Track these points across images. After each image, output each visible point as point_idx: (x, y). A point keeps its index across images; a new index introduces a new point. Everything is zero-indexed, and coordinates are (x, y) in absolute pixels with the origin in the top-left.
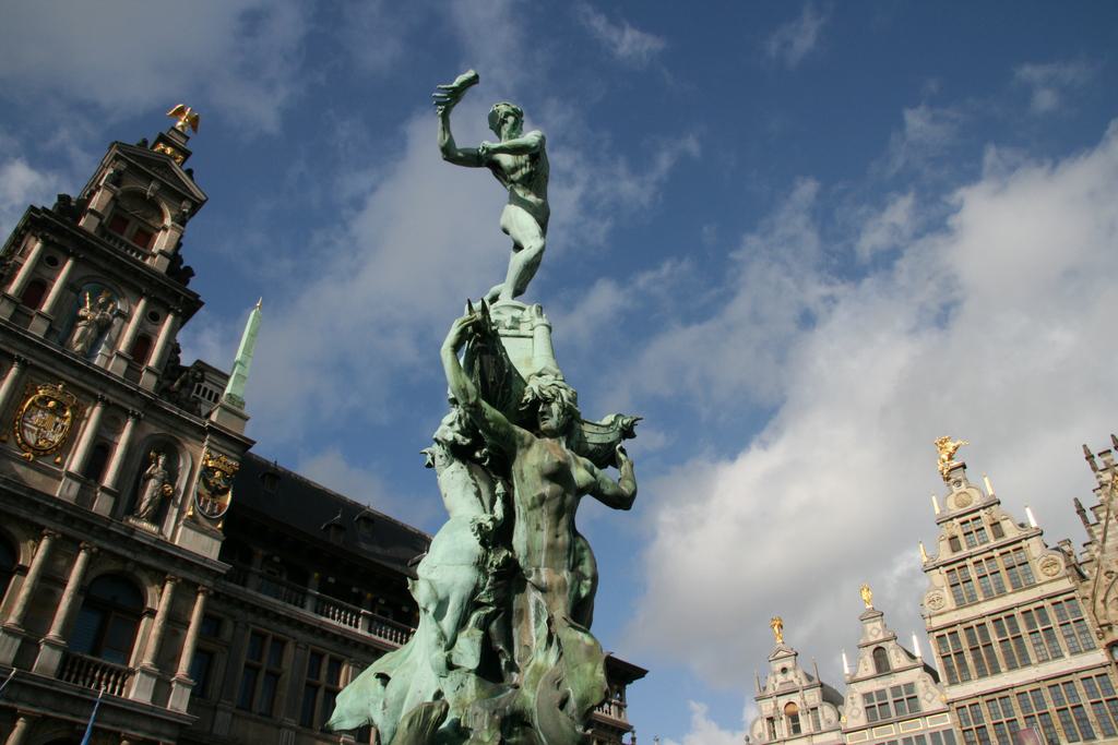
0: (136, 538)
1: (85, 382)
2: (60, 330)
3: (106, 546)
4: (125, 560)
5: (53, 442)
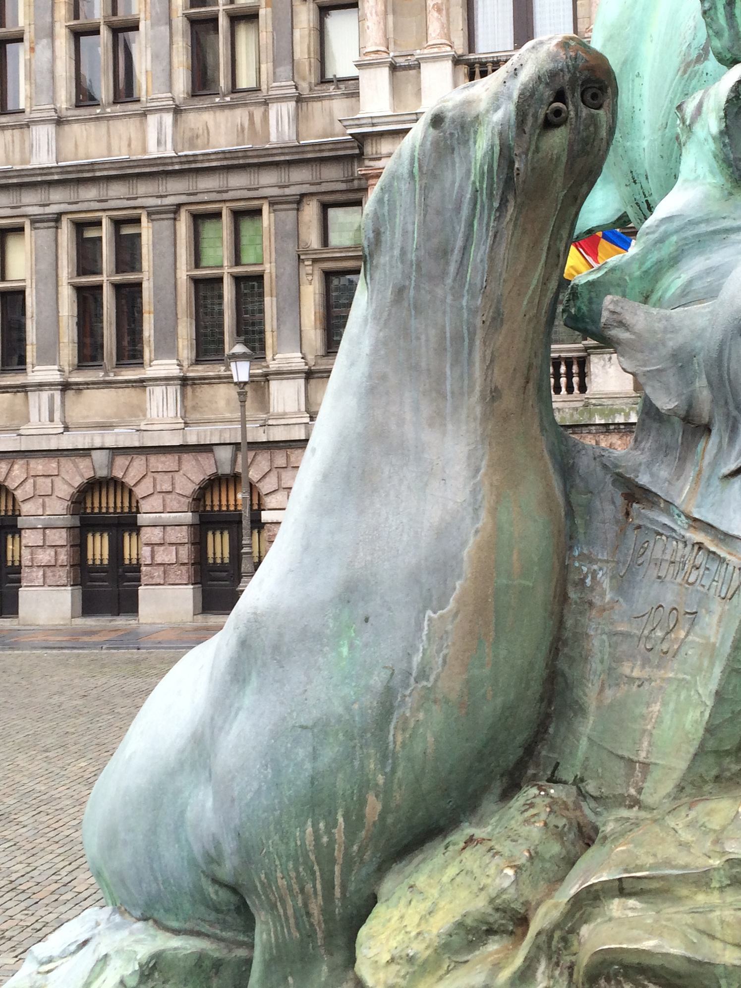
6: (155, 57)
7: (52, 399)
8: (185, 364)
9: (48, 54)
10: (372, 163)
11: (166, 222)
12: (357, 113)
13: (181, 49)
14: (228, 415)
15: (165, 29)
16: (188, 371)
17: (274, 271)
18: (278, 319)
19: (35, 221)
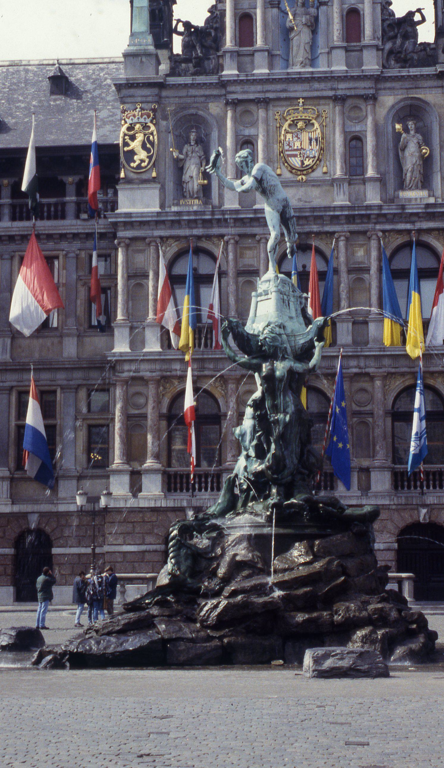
0: (407, 211)
1: (317, 90)
2: (278, 53)
3: (388, 227)
4: (409, 231)
5: (314, 157)
8: (12, 470)
10: (120, 374)
11: (4, 395)
12: (113, 348)
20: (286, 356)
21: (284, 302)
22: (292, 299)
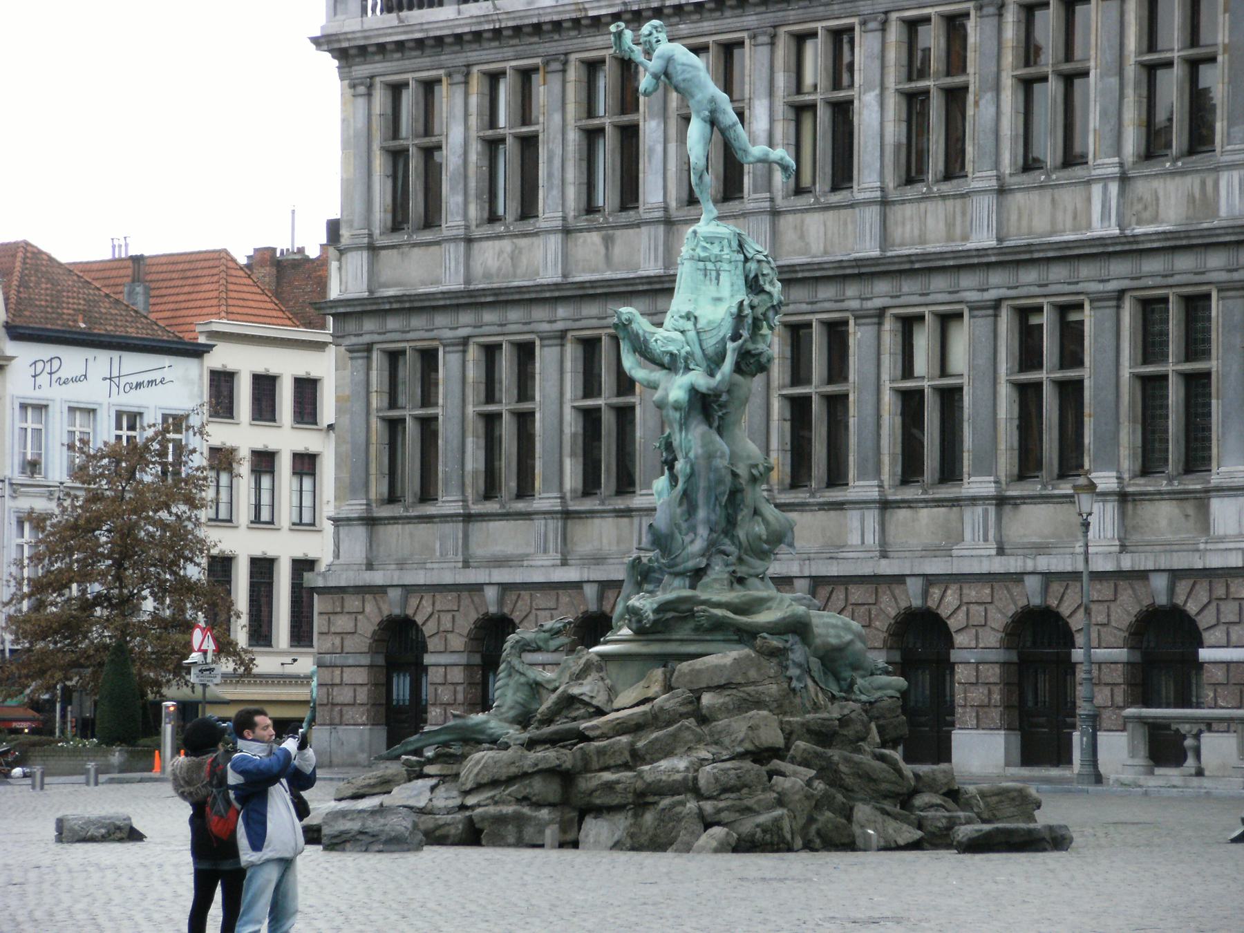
6: (1104, 113)
7: (986, 512)
9: (992, 110)
11: (1108, 311)
13: (1132, 104)
14: (1169, 537)
15: (1114, 81)
16: (1129, 485)
17: (1220, 369)
18: (1223, 426)
19: (974, 307)
20: (692, 366)
21: (706, 275)
22: (726, 266)
